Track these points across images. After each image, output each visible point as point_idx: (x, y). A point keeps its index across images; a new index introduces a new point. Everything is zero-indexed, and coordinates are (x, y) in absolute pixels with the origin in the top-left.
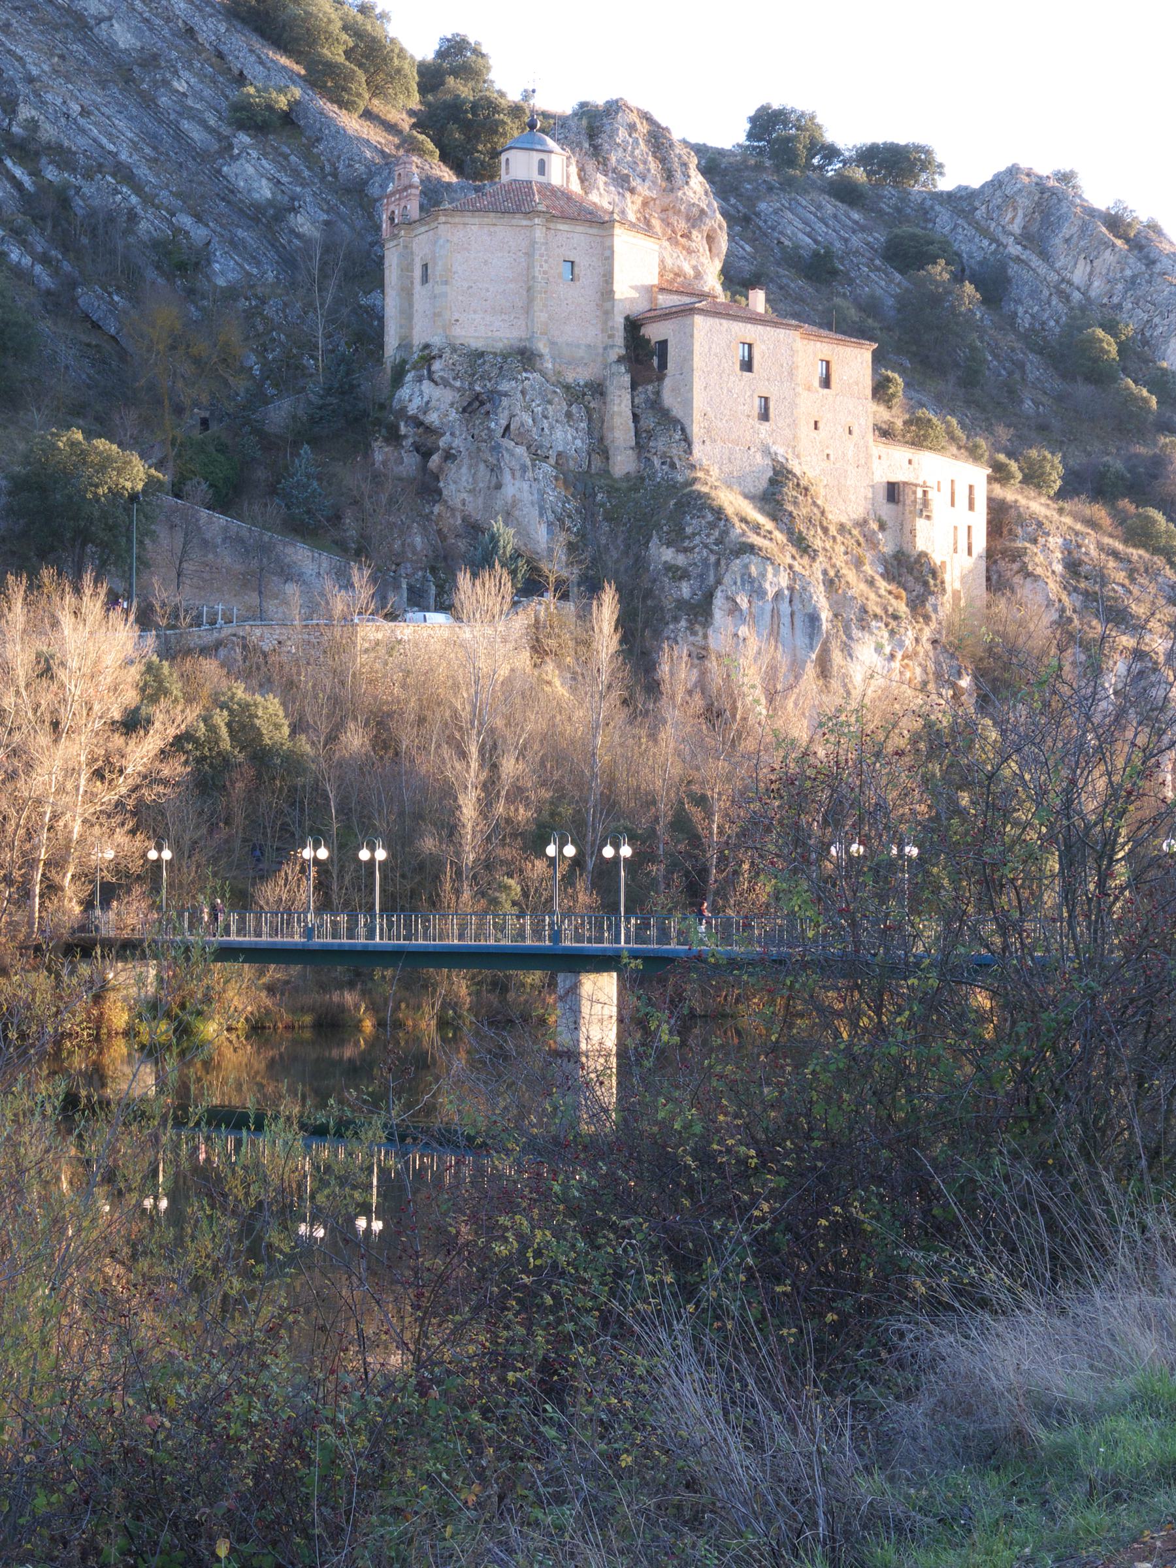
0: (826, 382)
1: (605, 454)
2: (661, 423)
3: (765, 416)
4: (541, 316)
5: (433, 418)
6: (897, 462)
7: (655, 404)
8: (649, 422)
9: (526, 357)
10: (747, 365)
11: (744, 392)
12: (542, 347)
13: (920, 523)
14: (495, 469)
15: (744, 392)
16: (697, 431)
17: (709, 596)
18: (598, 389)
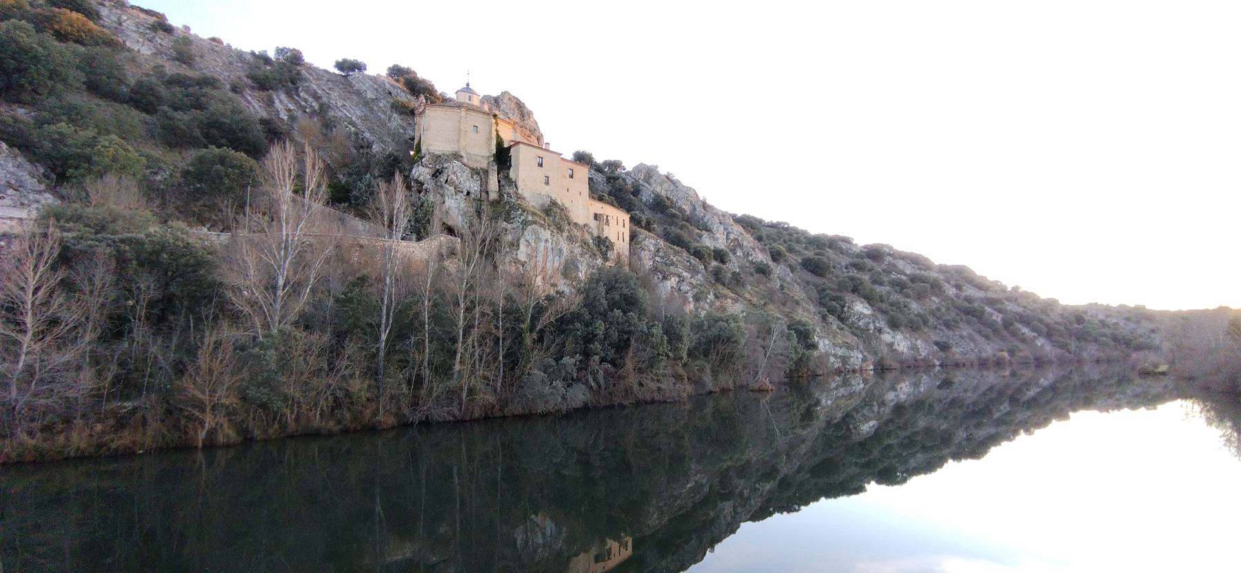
0: (571, 177)
1: (487, 193)
2: (506, 180)
3: (547, 183)
4: (463, 143)
5: (421, 178)
6: (599, 207)
7: (507, 177)
8: (503, 182)
9: (457, 156)
10: (541, 165)
11: (540, 174)
12: (463, 154)
13: (605, 227)
14: (442, 196)
15: (540, 174)
16: (520, 184)
17: (518, 240)
18: (486, 172)
